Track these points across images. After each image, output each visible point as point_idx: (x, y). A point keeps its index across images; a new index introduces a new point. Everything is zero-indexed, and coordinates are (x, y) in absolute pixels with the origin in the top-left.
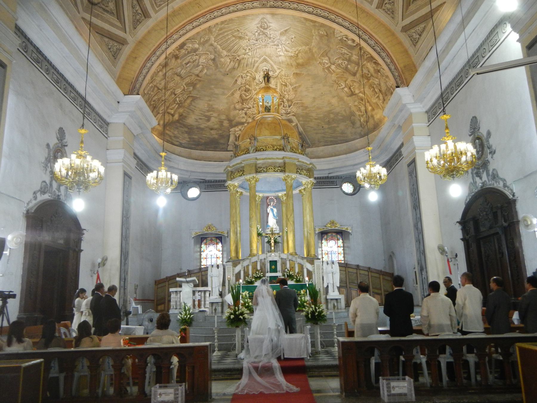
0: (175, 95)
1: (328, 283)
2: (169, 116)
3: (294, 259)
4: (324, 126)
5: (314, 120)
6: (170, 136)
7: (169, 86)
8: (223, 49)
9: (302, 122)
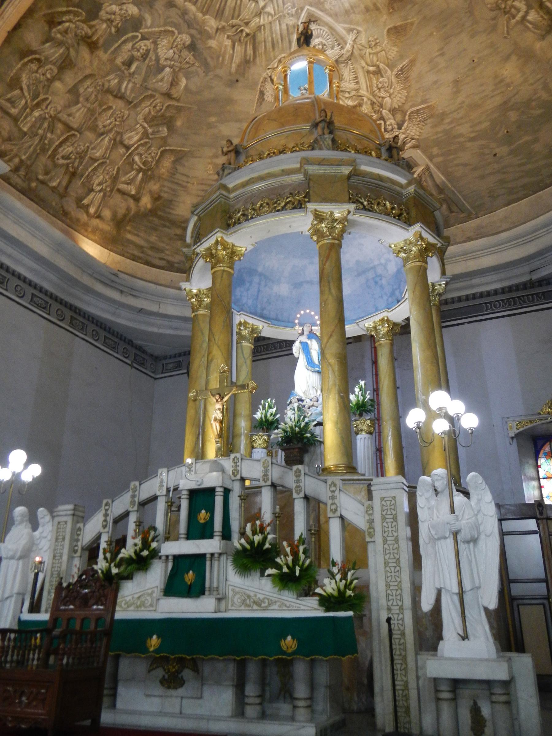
0: (127, 148)
1: (439, 593)
2: (125, 200)
3: (290, 480)
4: (497, 151)
5: (469, 144)
6: (140, 248)
7: (101, 127)
8: (204, 14)
9: (440, 159)
